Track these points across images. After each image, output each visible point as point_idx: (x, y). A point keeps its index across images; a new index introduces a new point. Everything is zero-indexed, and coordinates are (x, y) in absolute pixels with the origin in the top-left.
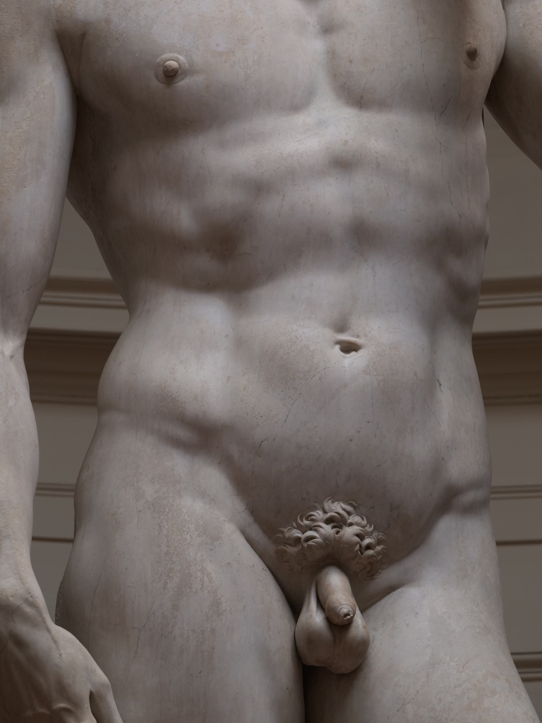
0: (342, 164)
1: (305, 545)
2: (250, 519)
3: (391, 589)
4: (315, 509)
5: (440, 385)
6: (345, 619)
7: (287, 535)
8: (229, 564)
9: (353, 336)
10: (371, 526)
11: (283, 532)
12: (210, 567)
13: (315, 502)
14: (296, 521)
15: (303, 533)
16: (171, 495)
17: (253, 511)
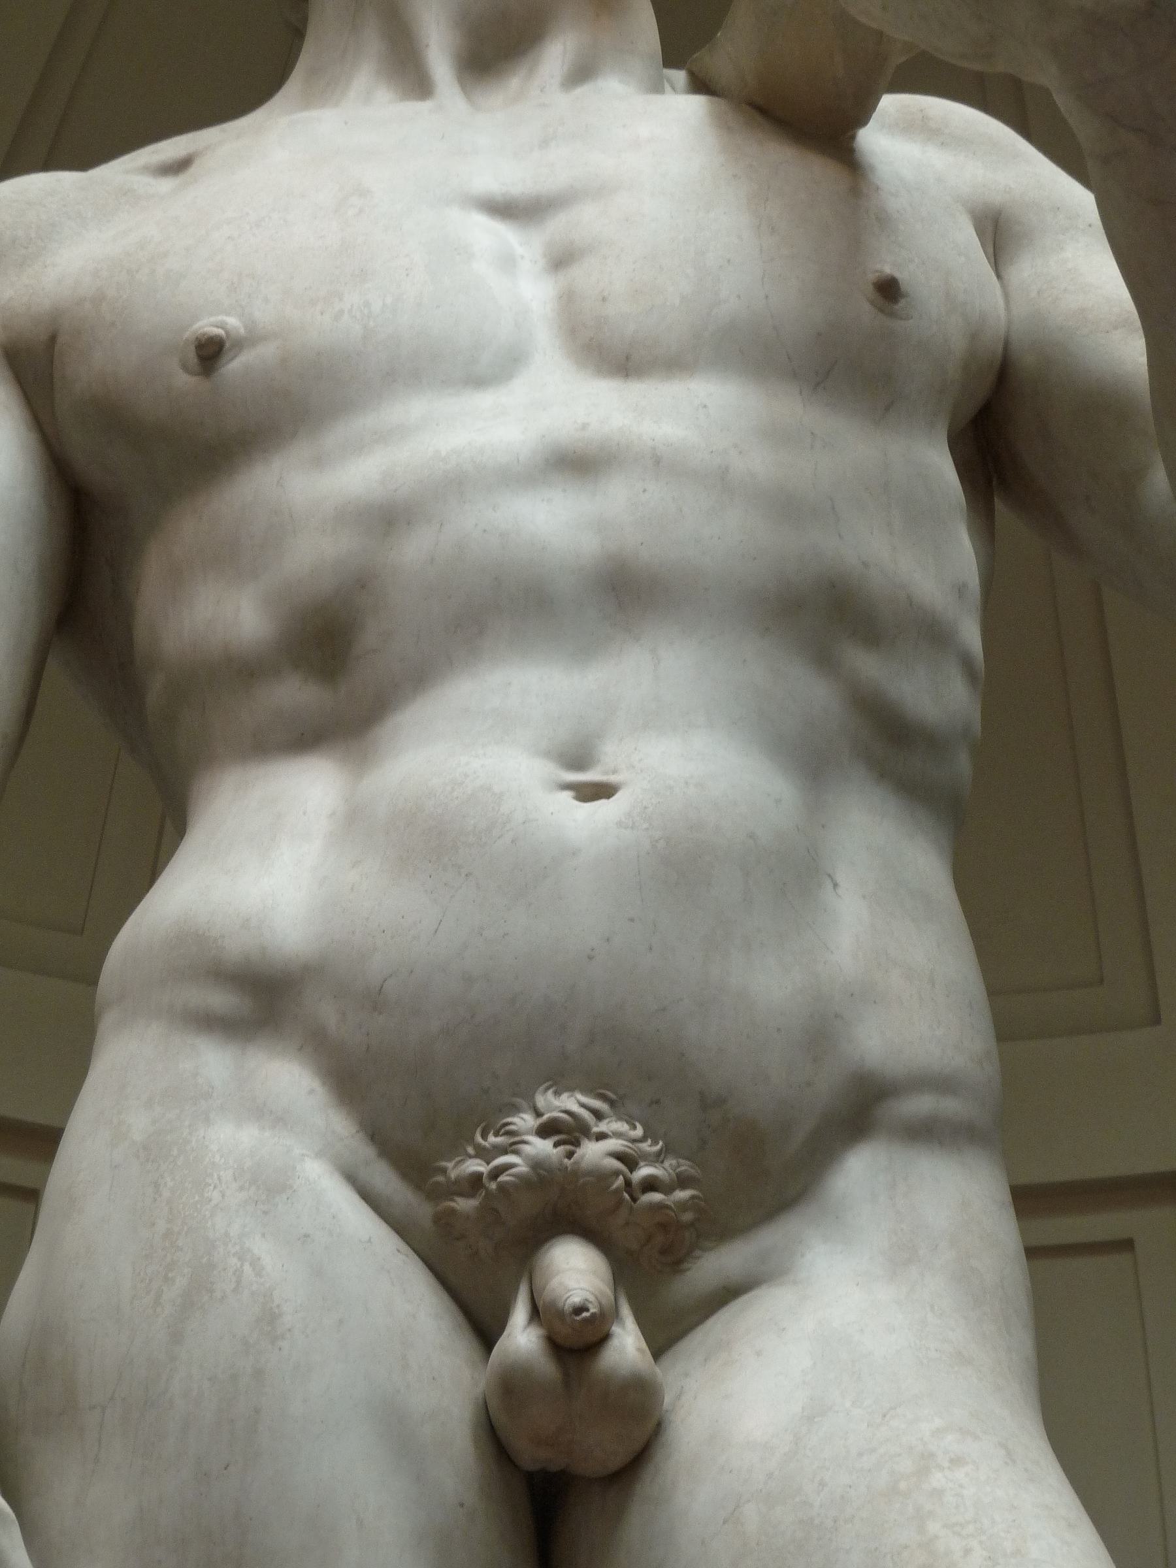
0: (576, 464)
1: (493, 1186)
2: (368, 1151)
3: (728, 1293)
4: (515, 1109)
5: (835, 885)
6: (578, 1318)
7: (453, 1175)
8: (307, 1236)
9: (606, 773)
10: (655, 1143)
11: (444, 1171)
12: (261, 1247)
13: (515, 1095)
14: (471, 1141)
15: (488, 1163)
16: (187, 1123)
17: (377, 1135)
